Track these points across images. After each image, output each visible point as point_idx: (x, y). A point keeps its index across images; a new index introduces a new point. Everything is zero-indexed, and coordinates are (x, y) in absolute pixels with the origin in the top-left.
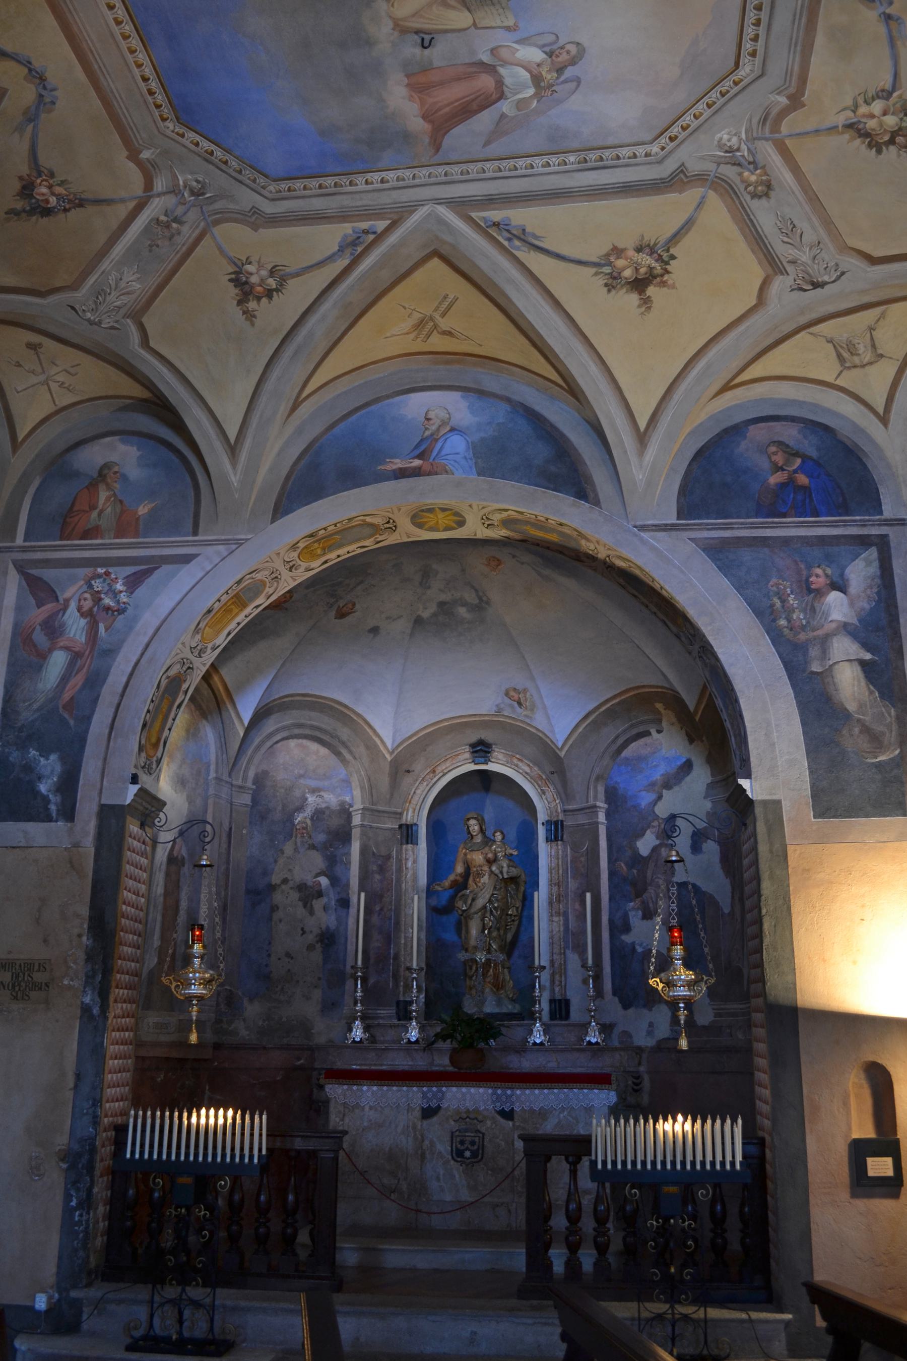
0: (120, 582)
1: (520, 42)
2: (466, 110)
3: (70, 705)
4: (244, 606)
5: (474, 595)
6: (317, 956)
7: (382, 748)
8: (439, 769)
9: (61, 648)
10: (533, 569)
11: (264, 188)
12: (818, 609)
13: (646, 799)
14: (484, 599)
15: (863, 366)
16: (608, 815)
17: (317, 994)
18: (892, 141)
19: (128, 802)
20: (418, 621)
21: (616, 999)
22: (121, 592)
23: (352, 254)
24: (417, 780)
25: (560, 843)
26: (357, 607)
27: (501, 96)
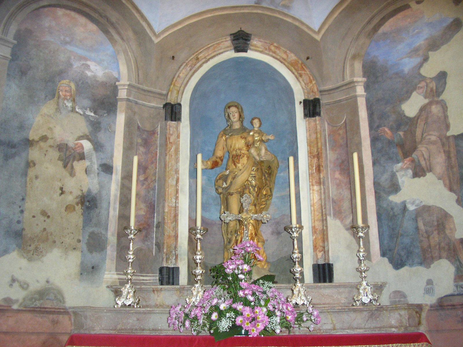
6: (76, 218)
7: (148, 31)
16: (367, 88)
21: (386, 260)
24: (181, 65)
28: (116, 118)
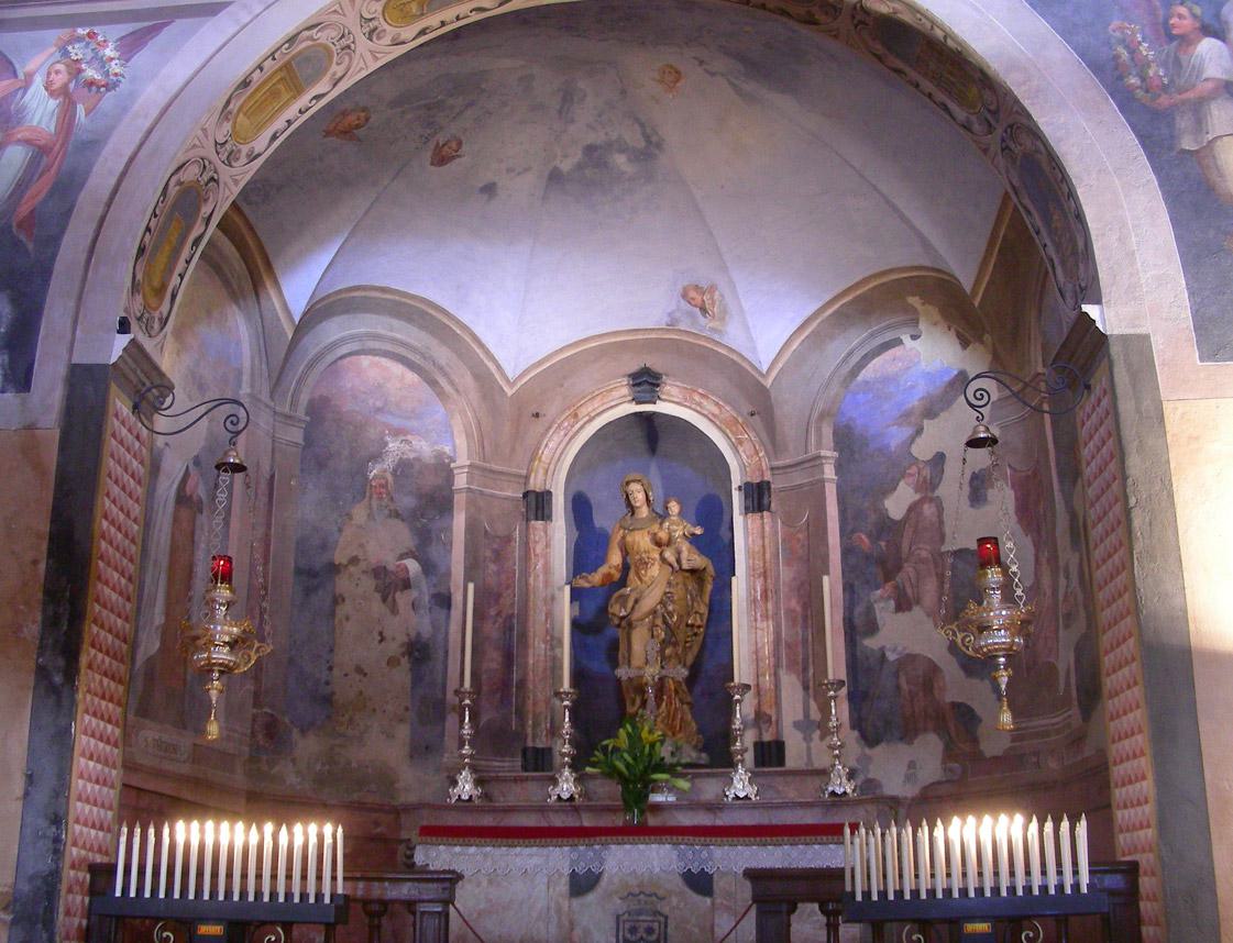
0: (111, 45)
3: (29, 222)
4: (298, 91)
5: (639, 136)
6: (402, 675)
7: (498, 376)
8: (583, 411)
9: (19, 141)
10: (731, 83)
12: (1184, 64)
13: (896, 436)
14: (654, 139)
16: (839, 468)
17: (403, 732)
19: (113, 360)
20: (555, 177)
21: (856, 733)
22: (112, 59)
24: (550, 428)
25: (765, 513)
26: (465, 148)
28: (452, 520)
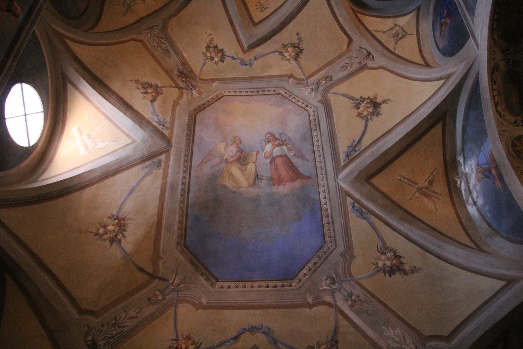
1: (263, 150)
2: (292, 167)
11: (329, 248)
15: (402, 28)
18: (298, 47)
23: (368, 214)
27: (286, 156)
